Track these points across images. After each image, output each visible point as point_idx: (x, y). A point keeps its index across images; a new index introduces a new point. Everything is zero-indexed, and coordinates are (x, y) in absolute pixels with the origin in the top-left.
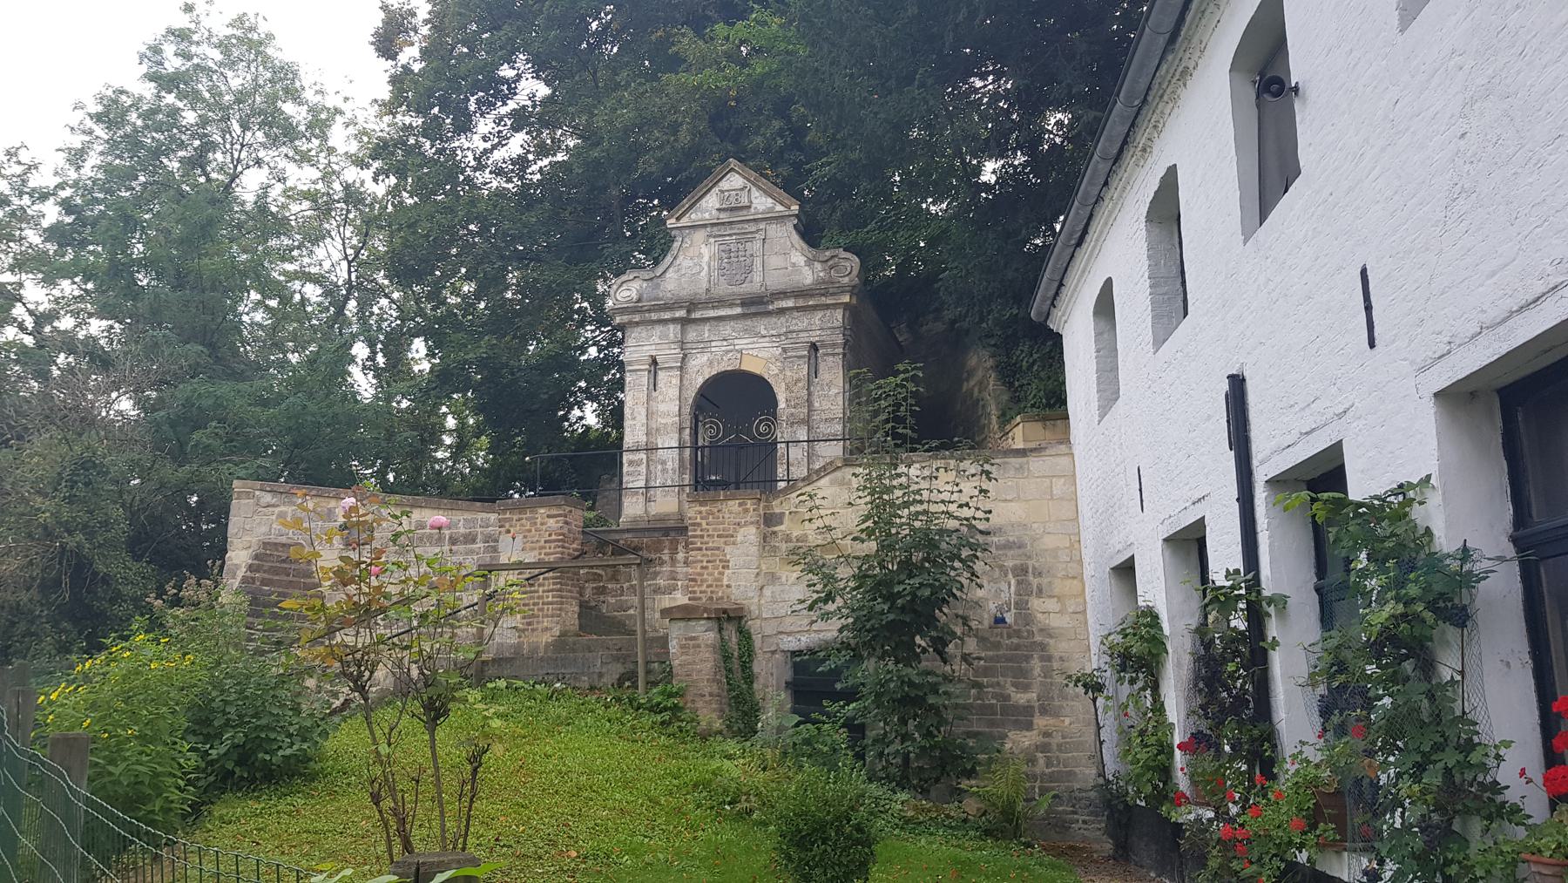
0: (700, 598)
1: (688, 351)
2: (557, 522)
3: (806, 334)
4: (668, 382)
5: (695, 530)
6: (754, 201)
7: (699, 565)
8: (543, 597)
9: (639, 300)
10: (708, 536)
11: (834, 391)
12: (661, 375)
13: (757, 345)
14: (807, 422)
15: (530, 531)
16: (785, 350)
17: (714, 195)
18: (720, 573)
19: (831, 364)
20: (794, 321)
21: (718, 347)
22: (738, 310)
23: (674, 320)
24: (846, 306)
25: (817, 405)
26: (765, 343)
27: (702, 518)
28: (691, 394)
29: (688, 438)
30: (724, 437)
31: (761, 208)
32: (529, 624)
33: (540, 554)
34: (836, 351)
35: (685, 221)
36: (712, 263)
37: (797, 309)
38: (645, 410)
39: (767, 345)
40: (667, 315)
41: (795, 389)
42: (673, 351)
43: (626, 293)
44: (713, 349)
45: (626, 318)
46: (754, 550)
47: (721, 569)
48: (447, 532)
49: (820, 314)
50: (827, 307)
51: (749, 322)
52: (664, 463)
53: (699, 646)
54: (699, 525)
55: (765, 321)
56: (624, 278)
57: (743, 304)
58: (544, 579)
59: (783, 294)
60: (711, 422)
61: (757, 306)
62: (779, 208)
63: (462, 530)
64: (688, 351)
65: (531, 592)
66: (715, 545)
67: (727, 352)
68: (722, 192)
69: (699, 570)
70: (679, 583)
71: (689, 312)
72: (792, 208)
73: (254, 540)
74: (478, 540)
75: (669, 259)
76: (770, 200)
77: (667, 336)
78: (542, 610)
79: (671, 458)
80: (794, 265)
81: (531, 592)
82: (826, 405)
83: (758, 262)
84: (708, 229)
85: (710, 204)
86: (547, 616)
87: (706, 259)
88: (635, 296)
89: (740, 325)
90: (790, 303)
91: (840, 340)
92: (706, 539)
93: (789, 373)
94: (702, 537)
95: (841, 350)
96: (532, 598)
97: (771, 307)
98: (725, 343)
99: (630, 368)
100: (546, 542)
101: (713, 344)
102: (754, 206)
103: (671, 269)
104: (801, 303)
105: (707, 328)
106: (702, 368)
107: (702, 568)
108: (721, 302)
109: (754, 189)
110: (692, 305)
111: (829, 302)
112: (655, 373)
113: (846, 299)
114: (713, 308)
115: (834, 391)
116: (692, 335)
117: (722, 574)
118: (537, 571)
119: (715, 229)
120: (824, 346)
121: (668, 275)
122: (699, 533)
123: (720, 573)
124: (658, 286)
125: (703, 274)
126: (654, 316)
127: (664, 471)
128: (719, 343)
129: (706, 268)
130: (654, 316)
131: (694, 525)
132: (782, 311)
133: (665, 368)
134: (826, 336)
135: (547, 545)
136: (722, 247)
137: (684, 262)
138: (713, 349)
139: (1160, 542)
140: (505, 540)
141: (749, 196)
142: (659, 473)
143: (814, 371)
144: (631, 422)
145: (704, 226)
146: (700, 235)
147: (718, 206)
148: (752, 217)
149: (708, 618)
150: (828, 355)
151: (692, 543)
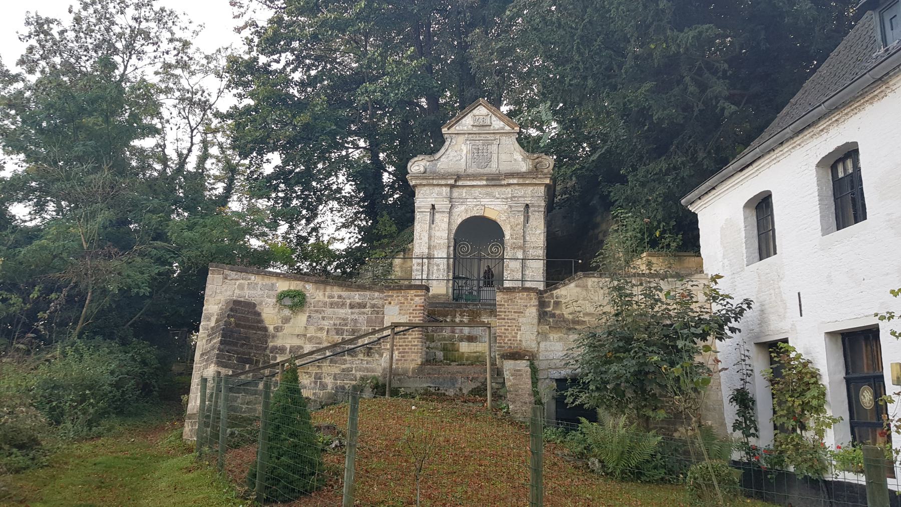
0: (504, 347)
1: (453, 203)
2: (421, 299)
3: (523, 199)
4: (442, 221)
5: (501, 308)
6: (493, 123)
7: (503, 328)
8: (411, 342)
9: (425, 172)
10: (509, 312)
11: (538, 232)
12: (437, 216)
13: (494, 203)
14: (523, 248)
15: (404, 303)
16: (511, 207)
17: (470, 117)
18: (515, 333)
19: (536, 216)
20: (516, 191)
21: (471, 202)
22: (484, 183)
23: (446, 185)
24: (546, 185)
25: (527, 238)
26: (498, 202)
27: (504, 302)
28: (454, 227)
29: (452, 252)
30: (470, 254)
31: (497, 127)
32: (403, 357)
33: (410, 317)
34: (540, 209)
35: (452, 130)
36: (468, 155)
37: (518, 184)
38: (427, 235)
39: (500, 203)
40: (443, 182)
41: (516, 229)
42: (445, 203)
43: (417, 168)
44: (468, 203)
45: (418, 182)
46: (536, 321)
47: (516, 331)
48: (348, 301)
49: (531, 188)
50: (536, 184)
51: (489, 190)
52: (438, 265)
53: (522, 375)
54: (504, 305)
55: (499, 189)
56: (416, 159)
57: (487, 180)
58: (412, 331)
59: (512, 175)
60: (464, 244)
61: (495, 180)
62: (507, 128)
63: (358, 301)
64: (453, 203)
65: (404, 338)
66: (513, 317)
67: (476, 205)
68: (475, 116)
69: (503, 331)
70: (457, 335)
71: (456, 181)
72: (515, 128)
73: (222, 299)
74: (367, 307)
75: (442, 150)
76: (502, 123)
77: (441, 194)
78: (411, 349)
79: (443, 264)
80: (515, 160)
81: (404, 338)
82: (534, 239)
83: (495, 156)
84: (466, 136)
85: (467, 122)
86: (413, 352)
87: (465, 152)
88: (422, 169)
90: (515, 181)
91: (543, 204)
92: (507, 313)
93: (513, 220)
94: (505, 312)
95: (543, 209)
96: (404, 342)
97: (503, 182)
98: (475, 200)
99: (419, 210)
100: (413, 310)
101: (468, 200)
102: (493, 125)
103: (443, 157)
104: (521, 181)
105: (465, 190)
106: (461, 214)
107: (505, 329)
108: (475, 177)
109: (493, 116)
110: (458, 177)
111: (537, 182)
112: (433, 214)
113: (547, 181)
114: (470, 180)
115: (538, 232)
116: (456, 193)
117: (517, 333)
118: (407, 328)
119: (470, 136)
120: (533, 206)
121: (442, 159)
122: (502, 310)
123: (515, 333)
124: (436, 165)
125: (462, 160)
126: (435, 182)
127: (438, 270)
128: (471, 200)
129: (464, 158)
131: (500, 305)
132: (509, 185)
133: (440, 212)
134: (535, 201)
135: (414, 312)
136: (474, 147)
137: (451, 153)
138: (468, 203)
139: (824, 334)
140: (387, 308)
141: (491, 120)
142: (435, 271)
143: (527, 219)
144: (419, 241)
145: (464, 134)
146: (461, 139)
147: (472, 123)
148: (492, 132)
149: (528, 360)
150: (535, 211)
151: (499, 315)
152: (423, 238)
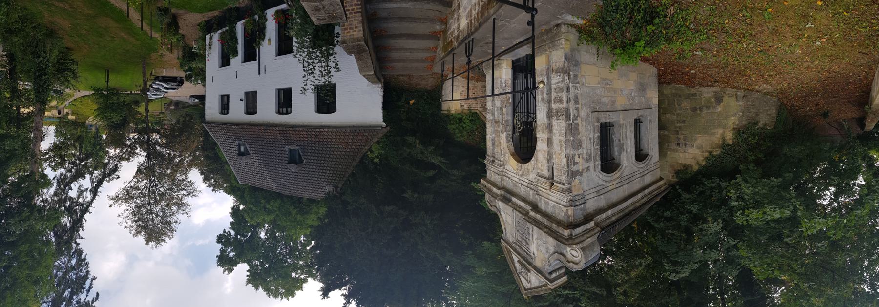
22: (514, 199)
42: (542, 189)
44: (527, 181)
89: (517, 190)
95: (487, 157)
97: (503, 192)
101: (526, 184)
138: (527, 181)
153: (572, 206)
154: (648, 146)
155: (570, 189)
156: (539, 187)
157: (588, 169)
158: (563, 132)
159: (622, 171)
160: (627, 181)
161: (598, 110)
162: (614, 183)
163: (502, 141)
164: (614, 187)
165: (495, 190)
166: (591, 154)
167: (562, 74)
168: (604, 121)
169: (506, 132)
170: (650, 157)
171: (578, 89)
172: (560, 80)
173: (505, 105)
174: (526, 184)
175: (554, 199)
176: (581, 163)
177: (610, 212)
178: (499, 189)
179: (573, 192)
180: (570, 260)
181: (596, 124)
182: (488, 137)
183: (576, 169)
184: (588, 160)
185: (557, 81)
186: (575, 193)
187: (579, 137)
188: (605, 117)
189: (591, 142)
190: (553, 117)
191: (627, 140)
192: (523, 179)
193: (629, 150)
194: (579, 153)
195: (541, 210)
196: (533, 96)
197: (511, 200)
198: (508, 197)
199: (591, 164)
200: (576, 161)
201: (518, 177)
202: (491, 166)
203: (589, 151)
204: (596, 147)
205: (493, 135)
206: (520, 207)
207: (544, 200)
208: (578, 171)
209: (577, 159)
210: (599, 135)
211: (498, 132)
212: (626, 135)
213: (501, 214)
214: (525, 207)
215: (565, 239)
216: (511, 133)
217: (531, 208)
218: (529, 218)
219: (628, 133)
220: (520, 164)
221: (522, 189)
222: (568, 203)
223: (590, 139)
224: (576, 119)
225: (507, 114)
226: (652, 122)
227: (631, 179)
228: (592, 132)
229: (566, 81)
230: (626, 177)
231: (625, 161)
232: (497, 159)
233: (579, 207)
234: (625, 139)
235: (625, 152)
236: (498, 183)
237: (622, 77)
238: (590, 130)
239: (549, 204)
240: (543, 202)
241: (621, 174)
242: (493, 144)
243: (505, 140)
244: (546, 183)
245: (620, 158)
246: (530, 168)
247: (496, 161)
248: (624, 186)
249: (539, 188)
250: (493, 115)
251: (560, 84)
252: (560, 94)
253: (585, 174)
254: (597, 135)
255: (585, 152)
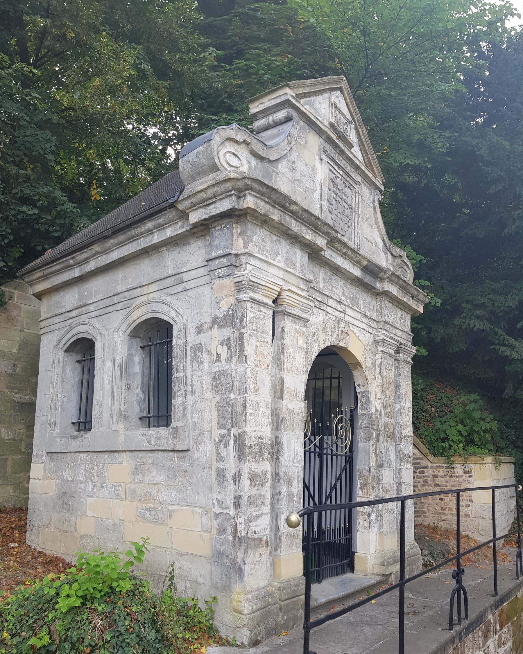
22: (357, 272)
44: (329, 310)
95: (410, 359)
101: (331, 302)
126: (295, 227)
130: (295, 227)
138: (329, 310)
152: (261, 390)
153: (236, 255)
154: (64, 371)
155: (239, 291)
156: (303, 297)
157: (199, 331)
158: (250, 410)
159: (128, 322)
160: (116, 299)
161: (176, 455)
162: (145, 298)
163: (379, 395)
164: (145, 290)
165: (394, 290)
166: (192, 361)
167: (249, 535)
168: (163, 431)
169: (371, 415)
170: (61, 345)
171: (218, 501)
172: (253, 524)
173: (371, 474)
174: (331, 302)
175: (273, 270)
176: (215, 343)
177: (156, 238)
178: (386, 294)
179: (232, 284)
180: (243, 146)
181: (180, 424)
182: (408, 403)
183: (224, 330)
184: (199, 347)
185: (259, 522)
186: (229, 282)
187: (218, 398)
188: (159, 438)
189: (192, 385)
190: (269, 442)
191: (112, 387)
192: (337, 313)
193: (109, 364)
194: (217, 364)
195: (302, 249)
196: (309, 491)
197: (362, 270)
198: (368, 276)
199: (192, 339)
200: (225, 348)
201: (347, 318)
202: (402, 341)
203: (196, 366)
204: (181, 374)
205: (398, 406)
206: (345, 255)
207: (294, 268)
208: (221, 327)
209: (223, 351)
210: (173, 401)
211: (389, 415)
212: (113, 399)
213: (383, 241)
214: (334, 255)
215: (252, 189)
216: (360, 411)
217: (323, 253)
218: (327, 234)
219: (107, 402)
220: (342, 344)
221: (339, 292)
222: (244, 261)
223: (193, 393)
224: (223, 436)
225: (367, 453)
226: (51, 423)
227: (107, 302)
228: (189, 407)
229: (242, 520)
230: (119, 307)
231: (119, 341)
232: (391, 355)
233: (220, 252)
234: (115, 388)
235: (118, 361)
236: (389, 305)
237: (115, 525)
238: (193, 413)
239: (286, 261)
240: (298, 265)
241: (128, 315)
242: (398, 387)
243: (372, 397)
244: (290, 305)
245: (129, 349)
246: (322, 337)
247: (392, 352)
248: (124, 289)
249: (304, 294)
250: (398, 452)
251: (255, 513)
252: (254, 492)
253: (207, 319)
254: (177, 401)
255: (206, 366)
